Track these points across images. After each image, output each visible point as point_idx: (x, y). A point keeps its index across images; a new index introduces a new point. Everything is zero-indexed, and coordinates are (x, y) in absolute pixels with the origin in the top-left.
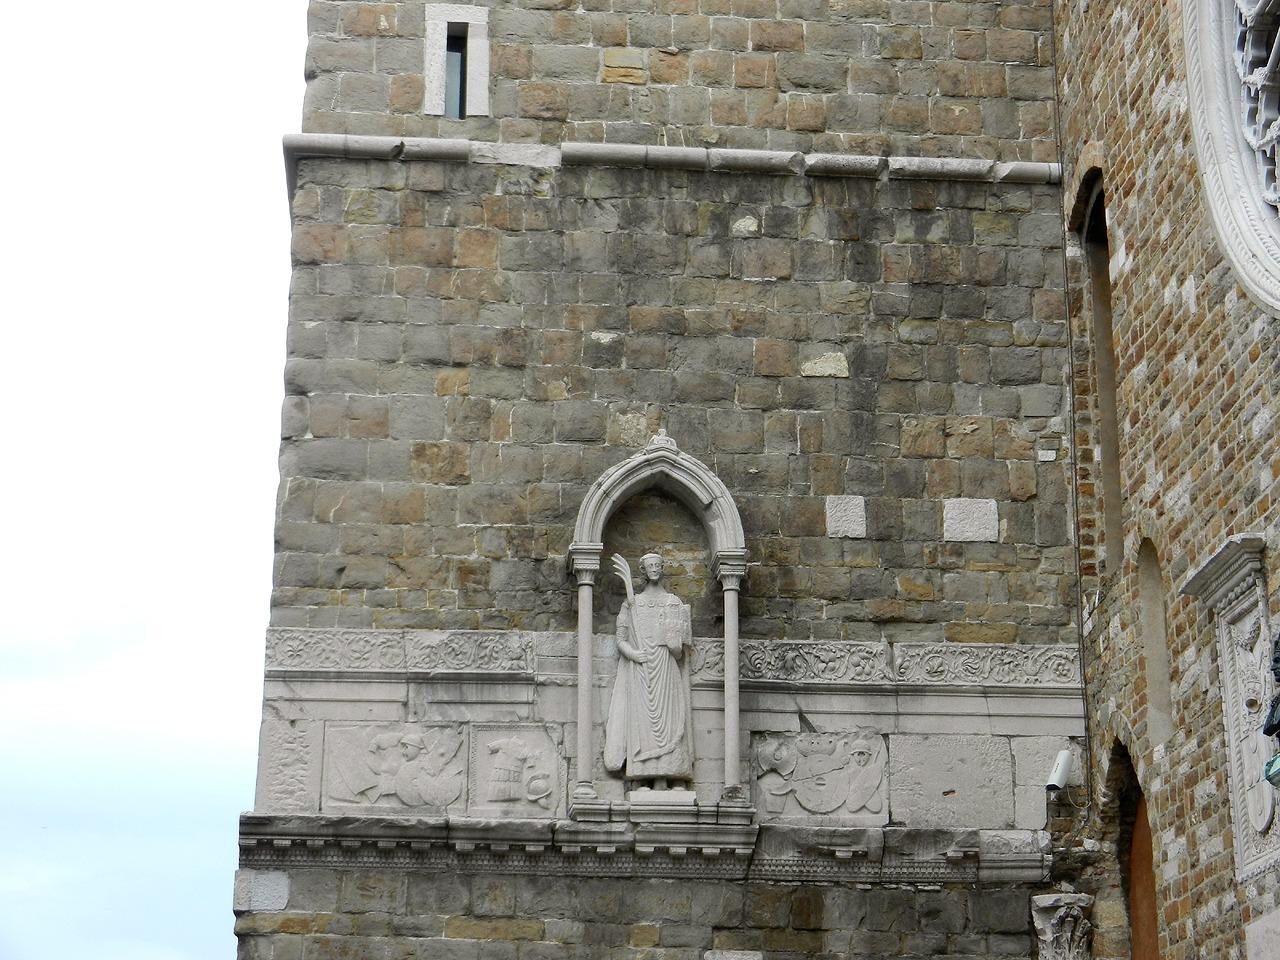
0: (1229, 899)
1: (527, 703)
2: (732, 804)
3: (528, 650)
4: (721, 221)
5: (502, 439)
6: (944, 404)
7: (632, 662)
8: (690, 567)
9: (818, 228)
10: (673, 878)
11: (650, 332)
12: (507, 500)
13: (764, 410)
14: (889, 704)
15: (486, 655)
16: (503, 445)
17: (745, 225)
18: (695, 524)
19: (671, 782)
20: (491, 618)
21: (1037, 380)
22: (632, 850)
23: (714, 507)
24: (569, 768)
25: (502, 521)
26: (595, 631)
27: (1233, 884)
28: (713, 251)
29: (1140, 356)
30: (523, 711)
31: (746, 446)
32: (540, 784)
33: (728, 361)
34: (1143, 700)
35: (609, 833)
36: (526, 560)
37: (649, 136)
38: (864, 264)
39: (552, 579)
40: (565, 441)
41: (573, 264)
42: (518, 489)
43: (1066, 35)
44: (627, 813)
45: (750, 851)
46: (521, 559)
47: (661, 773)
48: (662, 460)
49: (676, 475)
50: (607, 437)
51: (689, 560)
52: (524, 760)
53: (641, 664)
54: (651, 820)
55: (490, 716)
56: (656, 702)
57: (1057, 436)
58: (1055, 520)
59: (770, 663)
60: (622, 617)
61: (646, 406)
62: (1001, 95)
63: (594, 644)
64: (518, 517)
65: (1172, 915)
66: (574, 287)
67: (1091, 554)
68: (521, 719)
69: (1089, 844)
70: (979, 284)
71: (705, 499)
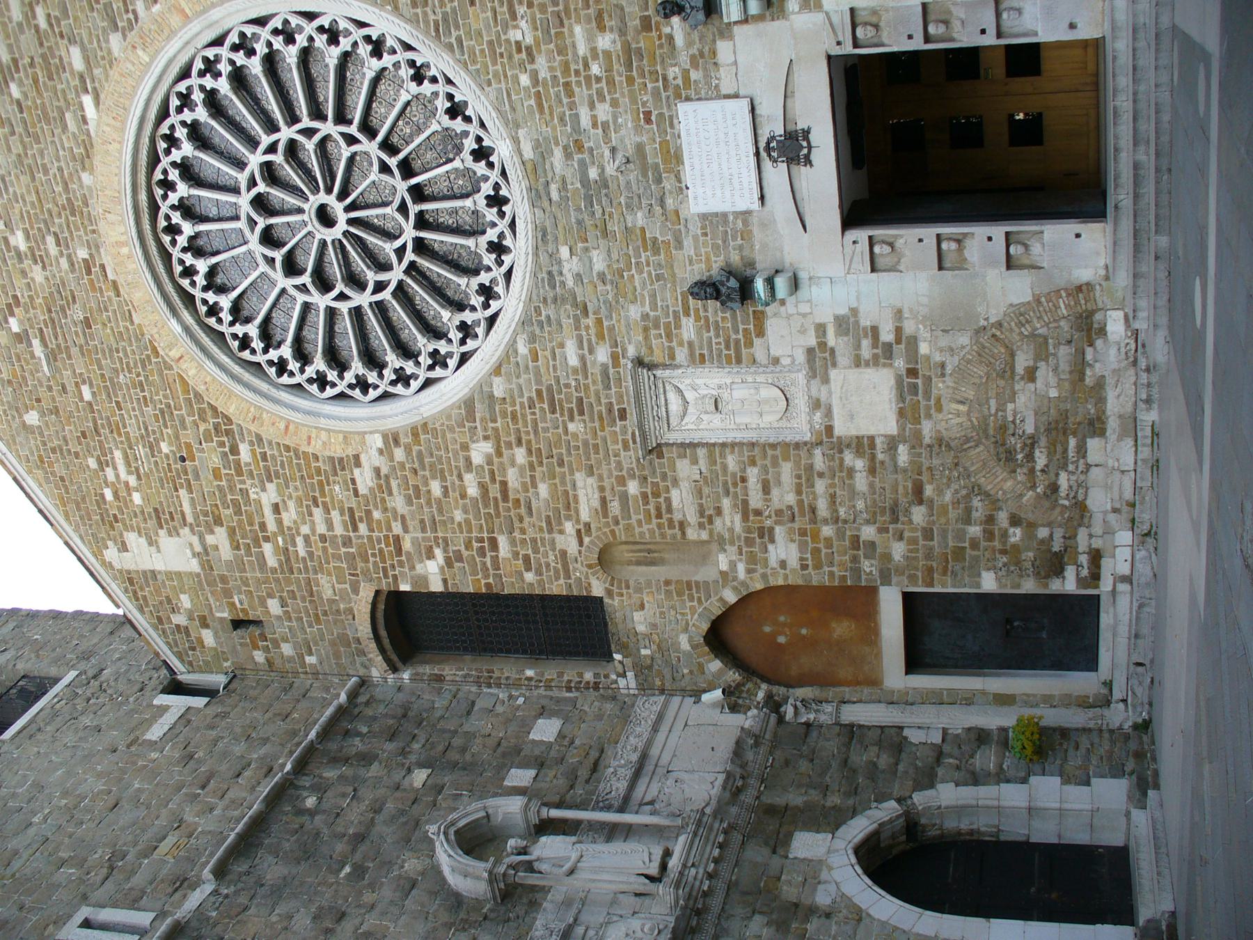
0: (819, 461)
4: (301, 812)
6: (470, 736)
7: (579, 864)
9: (330, 774)
11: (354, 850)
12: (435, 929)
14: (649, 768)
17: (311, 802)
19: (667, 854)
21: (473, 703)
23: (490, 811)
27: (809, 446)
28: (317, 818)
29: (494, 544)
33: (393, 818)
34: (689, 584)
37: (225, 839)
38: (366, 759)
41: (285, 881)
43: (287, 649)
44: (684, 866)
46: (480, 926)
48: (447, 828)
49: (461, 824)
50: (414, 877)
53: (582, 856)
57: (510, 697)
58: (558, 701)
62: (298, 701)
64: (448, 926)
65: (816, 551)
66: (302, 884)
67: (588, 683)
69: (761, 695)
70: (404, 716)
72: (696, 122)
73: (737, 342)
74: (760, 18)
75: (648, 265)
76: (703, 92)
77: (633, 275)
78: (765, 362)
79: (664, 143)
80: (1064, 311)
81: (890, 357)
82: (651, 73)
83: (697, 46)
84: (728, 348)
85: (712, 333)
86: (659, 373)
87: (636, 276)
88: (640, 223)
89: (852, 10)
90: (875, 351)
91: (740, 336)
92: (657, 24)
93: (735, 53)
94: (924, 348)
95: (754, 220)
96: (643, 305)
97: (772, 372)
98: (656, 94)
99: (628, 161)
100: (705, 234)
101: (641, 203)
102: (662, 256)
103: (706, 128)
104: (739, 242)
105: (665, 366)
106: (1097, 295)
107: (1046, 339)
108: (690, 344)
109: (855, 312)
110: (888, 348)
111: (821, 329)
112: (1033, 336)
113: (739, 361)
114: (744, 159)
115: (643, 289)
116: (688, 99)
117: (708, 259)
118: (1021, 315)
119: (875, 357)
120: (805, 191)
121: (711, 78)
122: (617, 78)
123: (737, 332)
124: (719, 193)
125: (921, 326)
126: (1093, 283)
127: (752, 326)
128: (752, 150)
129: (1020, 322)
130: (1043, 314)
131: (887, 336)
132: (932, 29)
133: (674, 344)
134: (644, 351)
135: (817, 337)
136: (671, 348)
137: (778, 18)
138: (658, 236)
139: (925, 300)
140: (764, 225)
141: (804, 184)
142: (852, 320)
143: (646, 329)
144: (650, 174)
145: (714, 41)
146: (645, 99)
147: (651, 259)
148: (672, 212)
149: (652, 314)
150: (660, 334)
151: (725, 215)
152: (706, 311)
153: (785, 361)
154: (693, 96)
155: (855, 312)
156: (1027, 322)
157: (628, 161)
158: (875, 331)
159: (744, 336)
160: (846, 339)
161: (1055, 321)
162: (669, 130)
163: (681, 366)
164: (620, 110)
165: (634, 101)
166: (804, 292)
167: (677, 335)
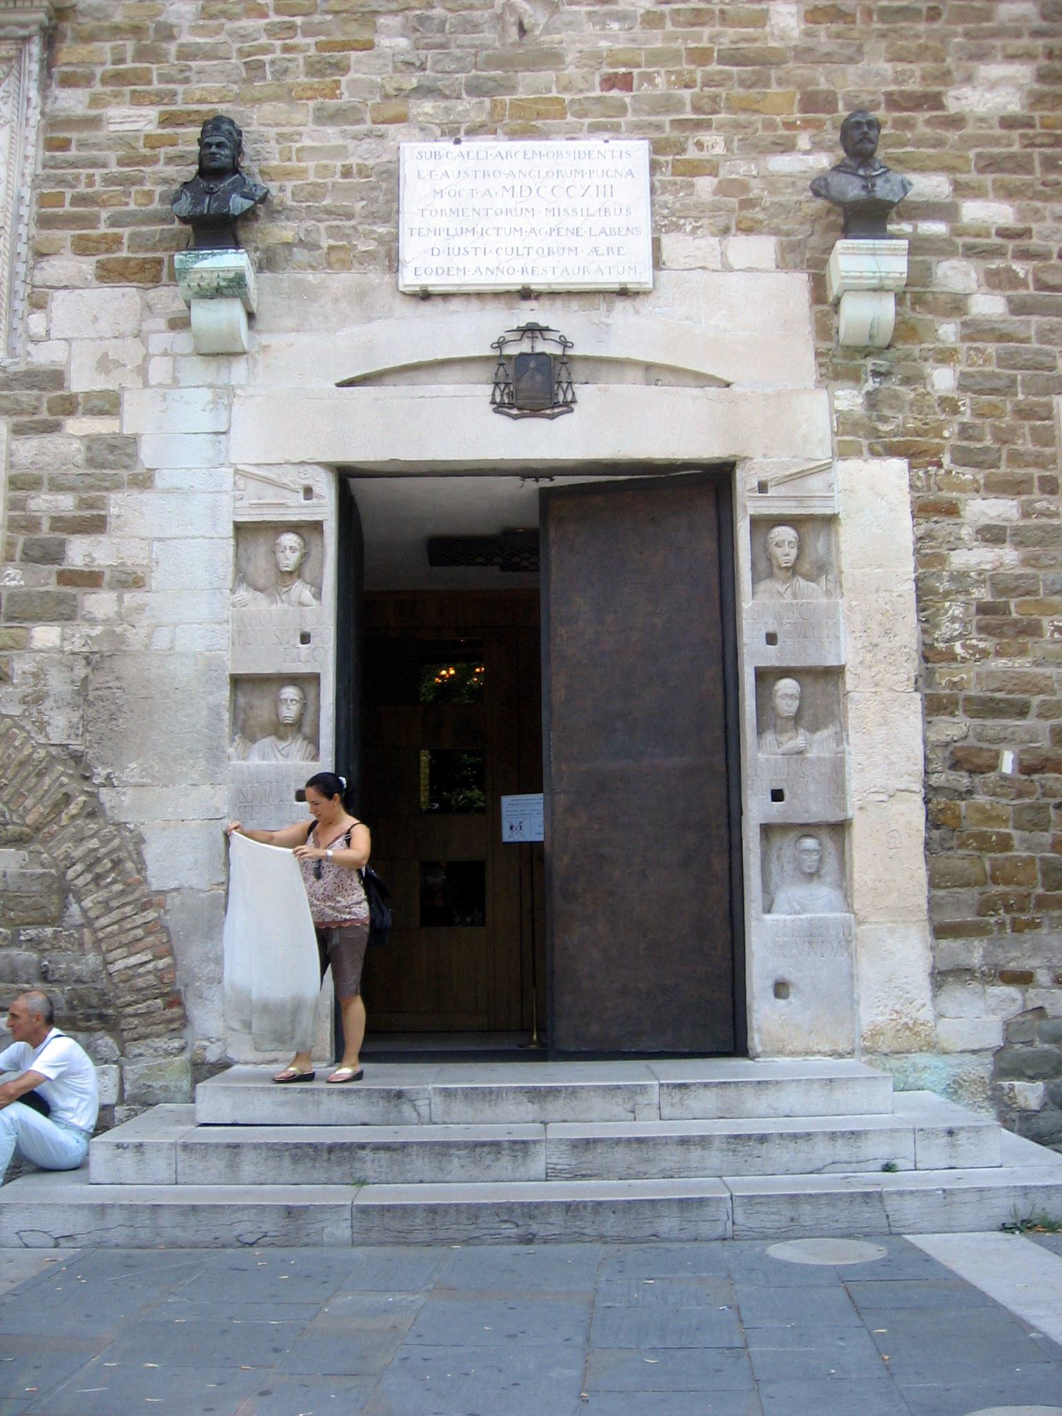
72: (606, 173)
73: (92, 221)
74: (824, 328)
75: (286, 49)
76: (668, 198)
77: (265, 16)
78: (39, 278)
79: (557, 109)
80: (120, 965)
81: (28, 558)
82: (714, 99)
83: (767, 199)
84: (79, 200)
85: (115, 169)
86: (35, 48)
87: (264, 22)
88: (384, 42)
89: (830, 521)
90: (46, 525)
91: (103, 229)
92: (819, 125)
93: (750, 270)
94: (46, 635)
95: (375, 277)
96: (195, 30)
97: (13, 292)
98: (668, 104)
99: (522, 30)
100: (347, 173)
101: (429, 47)
102: (303, 79)
103: (593, 190)
104: (326, 242)
105: (48, 65)
106: (162, 1043)
107: (56, 920)
108: (94, 123)
109: (144, 481)
110: (50, 554)
111: (108, 405)
112: (64, 890)
113: (45, 222)
114: (518, 263)
115: (231, 34)
116: (654, 167)
117: (288, 174)
118: (117, 863)
119: (32, 525)
120: (433, 389)
121: (697, 219)
122: (706, 31)
123: (115, 222)
124: (444, 203)
125: (98, 630)
126: (187, 1032)
127: (125, 254)
128: (537, 281)
129: (98, 860)
130: (115, 915)
131: (79, 552)
132: (787, 686)
133: (98, 87)
134: (89, 24)
135: (88, 394)
136: (88, 80)
137: (821, 365)
138: (352, 75)
139: (161, 641)
140: (361, 295)
141: (450, 389)
142: (125, 474)
143: (137, 31)
144: (493, 73)
145: (776, 232)
146: (658, 80)
147: (300, 57)
148: (402, 109)
149: (172, 48)
150: (122, 61)
151: (390, 213)
152: (170, 160)
153: (37, 322)
154: (658, 177)
155: (144, 481)
156: (98, 878)
157: (522, 30)
158: (95, 525)
159: (104, 236)
160: (80, 459)
161: (98, 942)
162: (587, 121)
163: (44, 98)
164: (637, 29)
165: (657, 58)
166: (195, 371)
167: (116, 95)
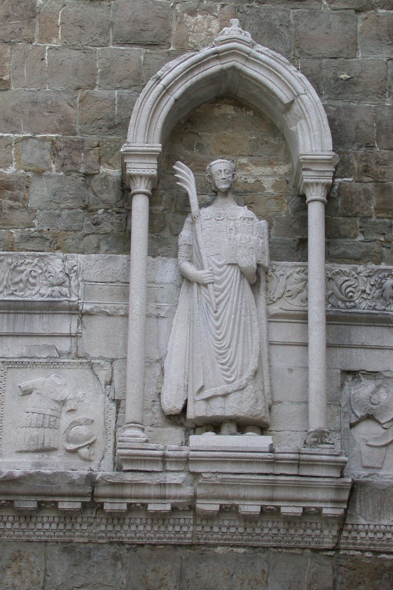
1: (70, 336)
2: (316, 450)
3: (73, 275)
5: (49, 41)
7: (195, 285)
8: (268, 183)
10: (244, 547)
12: (53, 109)
13: (358, 11)
15: (21, 280)
16: (50, 48)
18: (274, 137)
20: (30, 238)
22: (192, 508)
23: (295, 107)
24: (117, 412)
25: (46, 131)
26: (152, 253)
30: (65, 345)
31: (337, 50)
32: (83, 430)
35: (163, 485)
36: (75, 174)
39: (105, 196)
40: (123, 44)
42: (66, 96)
44: (187, 460)
45: (340, 512)
47: (229, 413)
48: (232, 52)
50: (172, 40)
51: (267, 176)
52: (63, 402)
53: (206, 285)
54: (215, 470)
55: (24, 351)
56: (223, 330)
59: (364, 291)
60: (185, 234)
61: (219, 7)
63: (149, 269)
68: (60, 354)
71: (285, 96)
